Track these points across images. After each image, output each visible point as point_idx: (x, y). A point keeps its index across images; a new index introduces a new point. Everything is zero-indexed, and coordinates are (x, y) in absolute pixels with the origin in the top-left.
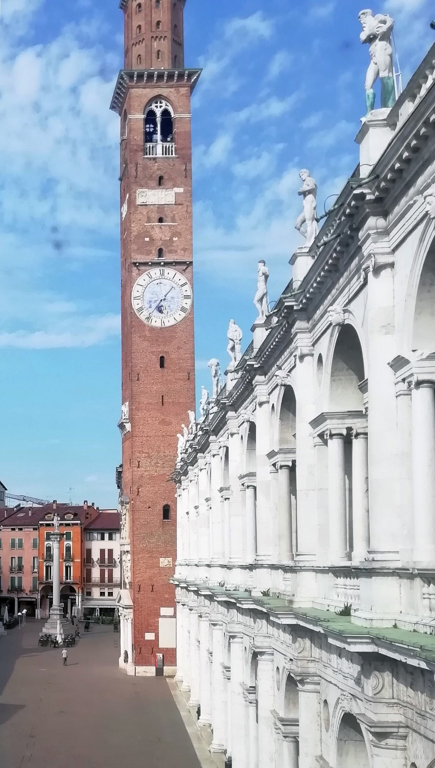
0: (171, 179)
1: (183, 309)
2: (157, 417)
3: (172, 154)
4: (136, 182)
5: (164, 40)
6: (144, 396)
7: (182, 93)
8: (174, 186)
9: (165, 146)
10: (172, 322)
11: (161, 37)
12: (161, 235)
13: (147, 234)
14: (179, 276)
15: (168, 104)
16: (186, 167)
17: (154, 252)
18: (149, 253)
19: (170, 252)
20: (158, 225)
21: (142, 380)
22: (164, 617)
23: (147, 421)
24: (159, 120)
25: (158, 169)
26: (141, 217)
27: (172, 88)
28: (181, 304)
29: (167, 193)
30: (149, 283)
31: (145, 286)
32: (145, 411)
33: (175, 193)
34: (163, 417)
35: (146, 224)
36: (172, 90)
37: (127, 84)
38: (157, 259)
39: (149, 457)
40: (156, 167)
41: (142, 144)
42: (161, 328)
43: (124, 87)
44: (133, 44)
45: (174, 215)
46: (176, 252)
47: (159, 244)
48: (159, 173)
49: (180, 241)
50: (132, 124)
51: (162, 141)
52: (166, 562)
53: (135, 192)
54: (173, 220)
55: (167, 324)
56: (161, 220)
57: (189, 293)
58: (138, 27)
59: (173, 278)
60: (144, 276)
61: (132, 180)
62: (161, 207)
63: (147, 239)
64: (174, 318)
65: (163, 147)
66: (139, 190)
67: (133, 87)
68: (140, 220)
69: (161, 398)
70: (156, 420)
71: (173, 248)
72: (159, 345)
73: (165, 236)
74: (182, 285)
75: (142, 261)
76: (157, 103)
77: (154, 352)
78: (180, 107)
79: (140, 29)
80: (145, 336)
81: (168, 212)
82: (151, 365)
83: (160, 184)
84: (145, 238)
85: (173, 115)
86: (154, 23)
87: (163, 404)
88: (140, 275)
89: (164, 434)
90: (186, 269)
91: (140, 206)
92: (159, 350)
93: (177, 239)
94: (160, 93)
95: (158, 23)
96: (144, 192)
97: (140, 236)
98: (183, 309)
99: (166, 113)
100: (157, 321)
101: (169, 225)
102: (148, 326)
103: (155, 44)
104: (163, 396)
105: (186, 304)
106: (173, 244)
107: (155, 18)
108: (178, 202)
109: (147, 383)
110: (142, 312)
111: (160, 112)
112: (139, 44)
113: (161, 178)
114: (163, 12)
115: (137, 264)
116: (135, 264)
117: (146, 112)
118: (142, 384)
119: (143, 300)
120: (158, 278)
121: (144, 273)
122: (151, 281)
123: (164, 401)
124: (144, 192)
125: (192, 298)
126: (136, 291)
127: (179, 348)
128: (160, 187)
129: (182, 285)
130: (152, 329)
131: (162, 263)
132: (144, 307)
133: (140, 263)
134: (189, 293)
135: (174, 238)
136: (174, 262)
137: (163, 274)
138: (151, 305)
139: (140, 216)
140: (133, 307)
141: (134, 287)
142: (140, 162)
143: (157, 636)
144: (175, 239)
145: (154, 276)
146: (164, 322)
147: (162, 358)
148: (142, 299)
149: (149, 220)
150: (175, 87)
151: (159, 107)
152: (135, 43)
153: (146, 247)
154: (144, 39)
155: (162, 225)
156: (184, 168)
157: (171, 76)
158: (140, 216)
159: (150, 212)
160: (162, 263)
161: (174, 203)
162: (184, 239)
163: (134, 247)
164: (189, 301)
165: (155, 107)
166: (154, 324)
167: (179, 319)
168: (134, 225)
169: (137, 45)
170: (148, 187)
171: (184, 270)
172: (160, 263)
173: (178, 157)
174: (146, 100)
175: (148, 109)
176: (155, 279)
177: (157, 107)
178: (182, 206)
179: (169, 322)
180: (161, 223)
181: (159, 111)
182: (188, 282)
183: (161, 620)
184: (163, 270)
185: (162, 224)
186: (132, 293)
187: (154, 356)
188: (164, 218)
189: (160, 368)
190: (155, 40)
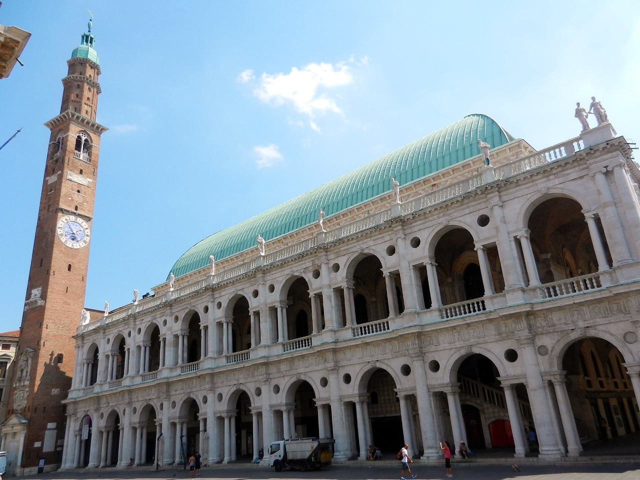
1: (85, 242)
8: (88, 177)
10: (78, 247)
19: (82, 209)
22: (50, 429)
24: (83, 142)
39: (54, 323)
46: (85, 210)
52: (56, 392)
55: (75, 247)
56: (79, 191)
61: (66, 165)
63: (70, 199)
67: (72, 120)
74: (87, 229)
81: (82, 189)
97: (66, 195)
98: (85, 242)
99: (86, 140)
100: (70, 244)
116: (62, 210)
129: (87, 229)
133: (65, 210)
134: (89, 234)
142: (72, 158)
143: (42, 444)
147: (70, 266)
149: (72, 190)
163: (61, 200)
166: (67, 245)
167: (82, 246)
175: (78, 135)
179: (76, 246)
183: (47, 432)
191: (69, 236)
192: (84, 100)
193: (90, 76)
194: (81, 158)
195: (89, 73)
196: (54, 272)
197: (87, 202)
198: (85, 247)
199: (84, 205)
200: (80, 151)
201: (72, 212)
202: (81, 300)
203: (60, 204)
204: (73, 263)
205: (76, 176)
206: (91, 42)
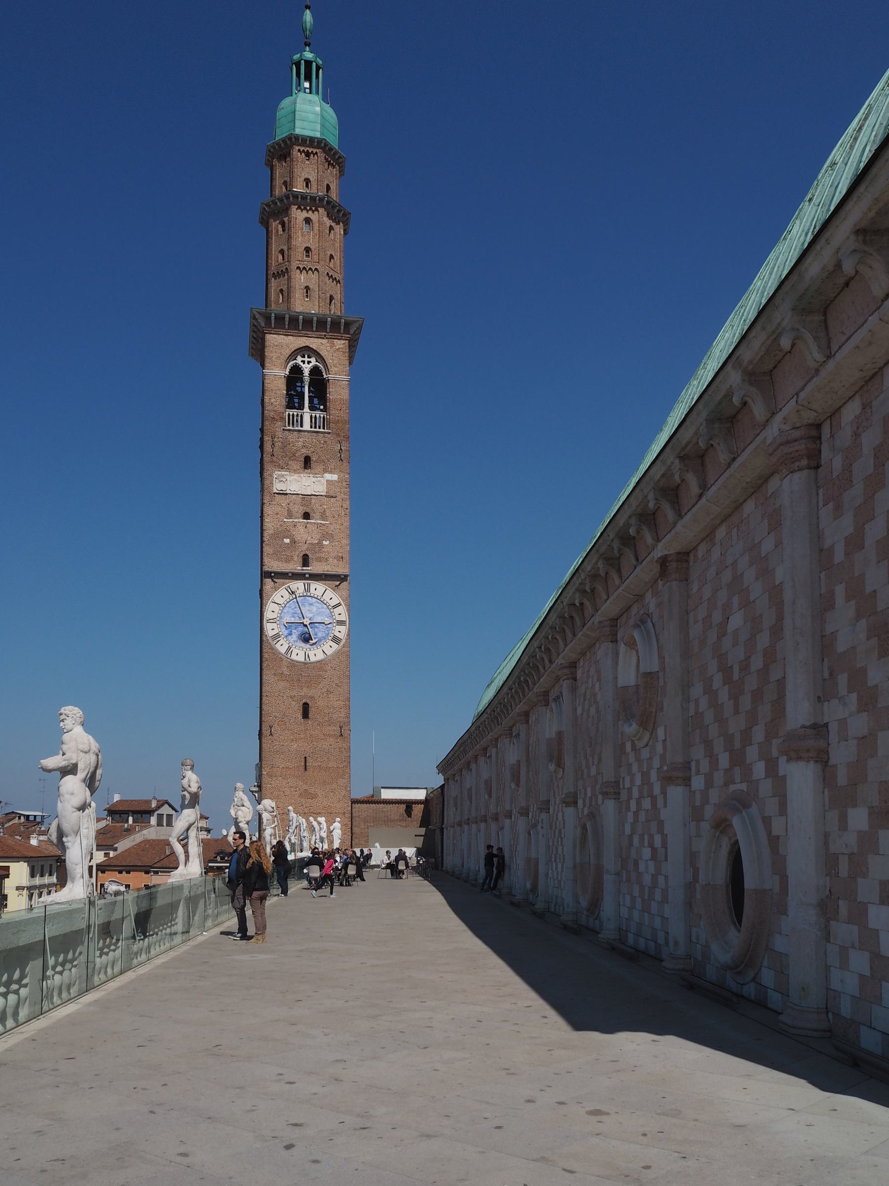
0: (320, 461)
1: (336, 640)
2: (296, 787)
4: (272, 462)
6: (279, 758)
7: (337, 347)
8: (325, 471)
9: (314, 415)
10: (320, 656)
12: (305, 536)
13: (287, 533)
14: (330, 593)
17: (296, 558)
18: (288, 560)
19: (319, 560)
20: (303, 522)
23: (284, 792)
25: (304, 446)
26: (280, 509)
27: (323, 338)
28: (333, 632)
29: (314, 479)
30: (288, 600)
31: (283, 605)
32: (280, 779)
33: (327, 481)
34: (305, 787)
35: (285, 520)
38: (300, 568)
40: (300, 444)
42: (305, 664)
45: (324, 511)
47: (303, 549)
49: (333, 546)
53: (271, 476)
54: (323, 516)
56: (306, 516)
57: (344, 617)
59: (322, 596)
60: (283, 591)
62: (306, 498)
63: (287, 541)
64: (323, 651)
65: (311, 417)
66: (276, 473)
69: (303, 760)
71: (323, 555)
74: (335, 607)
76: (303, 357)
77: (295, 696)
80: (282, 673)
84: (285, 539)
87: (306, 769)
88: (276, 589)
89: (306, 811)
90: (340, 584)
91: (275, 495)
92: (301, 694)
94: (307, 344)
96: (283, 476)
98: (336, 640)
99: (315, 371)
100: (299, 654)
101: (318, 524)
104: (305, 758)
105: (340, 632)
108: (331, 494)
117: (289, 367)
121: (283, 587)
123: (308, 764)
124: (283, 476)
128: (306, 471)
129: (335, 607)
130: (293, 664)
131: (307, 576)
132: (281, 633)
135: (324, 541)
137: (309, 590)
138: (291, 631)
142: (279, 434)
144: (324, 543)
146: (308, 656)
148: (278, 622)
149: (290, 515)
150: (327, 338)
151: (306, 362)
160: (307, 576)
162: (337, 543)
165: (302, 361)
166: (294, 657)
167: (329, 652)
170: (288, 470)
172: (305, 574)
174: (288, 352)
177: (304, 362)
179: (316, 655)
180: (307, 519)
181: (306, 368)
184: (309, 585)
185: (309, 521)
187: (294, 703)
188: (311, 514)
191: (294, 637)
192: (298, 254)
193: (307, 181)
194: (307, 426)
195: (305, 175)
196: (271, 727)
198: (337, 653)
200: (301, 407)
201: (293, 574)
202: (341, 781)
204: (312, 697)
205: (296, 476)
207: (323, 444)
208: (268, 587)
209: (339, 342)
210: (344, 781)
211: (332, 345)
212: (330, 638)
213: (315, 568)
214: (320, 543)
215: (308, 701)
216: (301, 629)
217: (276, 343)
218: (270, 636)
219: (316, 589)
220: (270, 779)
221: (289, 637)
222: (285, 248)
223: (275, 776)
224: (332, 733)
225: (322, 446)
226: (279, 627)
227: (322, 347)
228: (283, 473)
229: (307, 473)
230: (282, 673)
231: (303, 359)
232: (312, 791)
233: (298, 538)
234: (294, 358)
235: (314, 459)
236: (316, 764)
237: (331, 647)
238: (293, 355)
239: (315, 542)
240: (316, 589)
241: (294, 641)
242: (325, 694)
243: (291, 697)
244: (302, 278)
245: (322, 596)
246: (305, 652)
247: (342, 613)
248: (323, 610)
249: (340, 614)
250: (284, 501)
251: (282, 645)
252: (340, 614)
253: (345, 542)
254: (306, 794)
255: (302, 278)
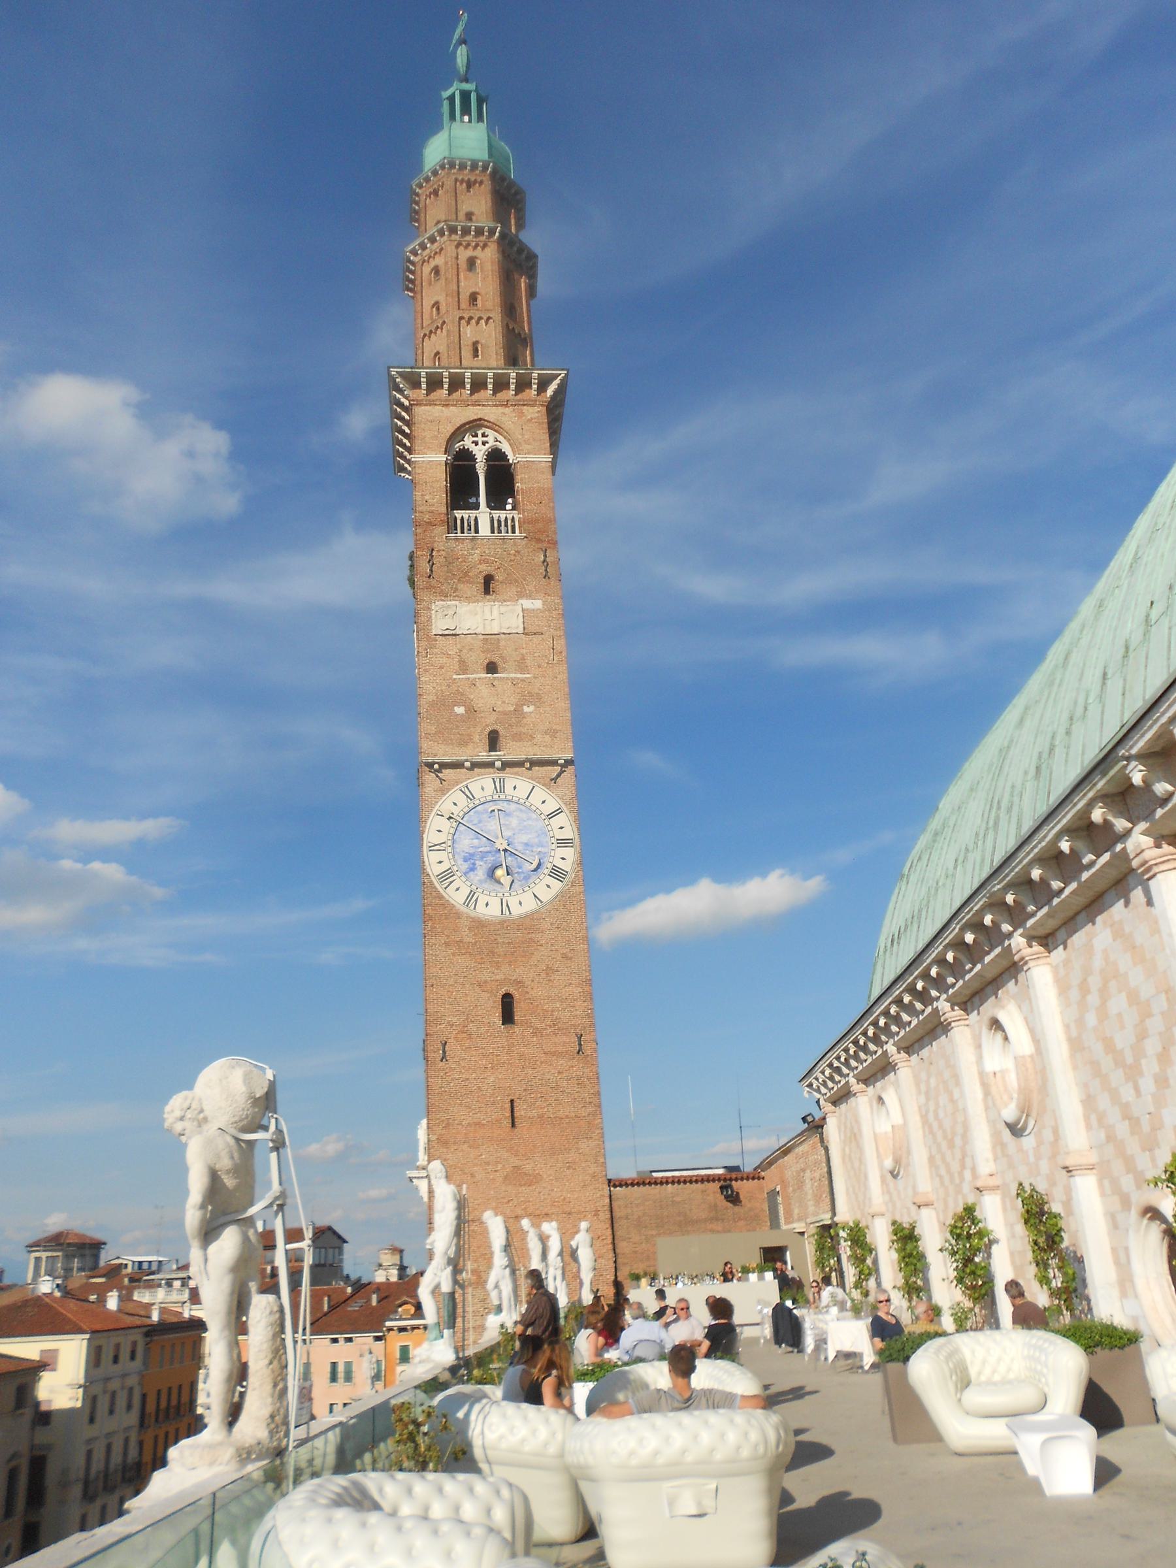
1: (557, 873)
2: (497, 1163)
3: (514, 532)
5: (486, 324)
6: (461, 1105)
8: (521, 595)
9: (496, 517)
10: (530, 905)
11: (480, 318)
14: (540, 794)
15: (500, 438)
16: (545, 556)
17: (476, 738)
18: (464, 741)
19: (518, 738)
20: (486, 678)
21: (456, 1059)
23: (472, 1175)
29: (503, 609)
30: (466, 810)
35: (455, 677)
36: (507, 410)
37: (406, 398)
38: (485, 754)
40: (476, 557)
41: (443, 509)
42: (502, 923)
43: (401, 405)
44: (425, 335)
45: (523, 658)
47: (490, 722)
48: (485, 569)
50: (420, 472)
51: (489, 506)
54: (522, 666)
55: (517, 911)
56: (492, 668)
57: (569, 833)
58: (433, 307)
59: (527, 798)
62: (490, 640)
63: (460, 710)
64: (535, 896)
68: (441, 668)
69: (508, 1106)
70: (496, 1171)
71: (524, 730)
72: (498, 965)
73: (504, 702)
74: (551, 816)
75: (447, 759)
77: (486, 982)
78: (527, 442)
79: (438, 309)
80: (461, 941)
82: (479, 1017)
83: (487, 591)
84: (456, 708)
85: (511, 458)
86: (465, 296)
87: (513, 1125)
88: (443, 792)
90: (559, 775)
93: (531, 708)
95: (473, 297)
97: (443, 703)
98: (557, 873)
99: (496, 456)
102: (468, 917)
103: (469, 332)
104: (512, 1101)
105: (563, 859)
106: (524, 720)
107: (467, 287)
108: (532, 629)
109: (470, 1068)
110: (451, 882)
111: (482, 452)
112: (435, 333)
113: (488, 580)
114: (484, 279)
115: (436, 766)
116: (430, 765)
118: (455, 1069)
119: (453, 852)
120: (489, 798)
121: (456, 789)
122: (471, 806)
123: (517, 1114)
125: (577, 842)
126: (435, 830)
127: (549, 970)
128: (488, 597)
129: (551, 816)
130: (479, 924)
131: (498, 764)
132: (455, 868)
133: (444, 766)
135: (525, 707)
136: (527, 760)
138: (474, 864)
139: (443, 660)
140: (429, 870)
141: (429, 822)
142: (440, 545)
144: (526, 709)
145: (478, 793)
146: (507, 905)
149: (464, 668)
151: (480, 443)
152: (428, 333)
153: (457, 727)
154: (444, 322)
155: (495, 678)
156: (542, 558)
157: (501, 384)
158: (443, 660)
159: (465, 651)
161: (521, 630)
162: (548, 709)
164: (570, 853)
166: (481, 909)
167: (546, 895)
168: (427, 679)
169: (433, 335)
171: (555, 780)
172: (491, 765)
173: (526, 537)
174: (451, 429)
176: (483, 800)
177: (476, 443)
178: (540, 637)
179: (523, 904)
182: (564, 808)
184: (502, 781)
186: (425, 836)
187: (486, 995)
188: (500, 665)
189: (503, 1024)
190: (468, 323)
191: (481, 873)
197: (536, 699)
198: (561, 894)
199: (523, 715)
200: (476, 506)
201: (475, 765)
202: (584, 1145)
203: (425, 745)
204: (519, 983)
206: (466, 110)
207: (515, 555)
208: (428, 789)
209: (531, 409)
210: (592, 1144)
211: (521, 414)
212: (546, 871)
213: (511, 751)
214: (518, 710)
215: (512, 991)
216: (490, 858)
217: (429, 418)
218: (436, 874)
219: (515, 788)
220: (445, 1150)
221: (471, 874)
222: (441, 299)
223: (455, 1143)
224: (560, 1049)
225: (513, 558)
226: (451, 857)
227: (504, 419)
228: (449, 603)
229: (489, 601)
230: (461, 941)
231: (475, 439)
232: (528, 1168)
233: (479, 704)
234: (460, 438)
235: (501, 579)
236: (534, 1113)
237: (548, 886)
238: (459, 433)
239: (509, 709)
240: (515, 788)
241: (480, 881)
242: (543, 975)
243: (480, 985)
244: (468, 332)
245: (527, 798)
246: (502, 900)
247: (565, 825)
248: (530, 822)
249: (561, 828)
250: (452, 647)
251: (457, 889)
252: (561, 828)
253: (563, 705)
254: (517, 1177)
255: (468, 332)
